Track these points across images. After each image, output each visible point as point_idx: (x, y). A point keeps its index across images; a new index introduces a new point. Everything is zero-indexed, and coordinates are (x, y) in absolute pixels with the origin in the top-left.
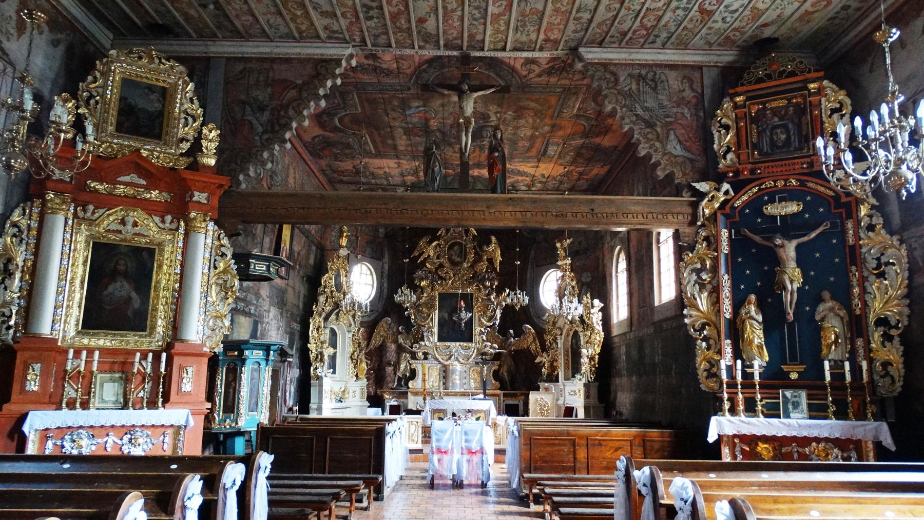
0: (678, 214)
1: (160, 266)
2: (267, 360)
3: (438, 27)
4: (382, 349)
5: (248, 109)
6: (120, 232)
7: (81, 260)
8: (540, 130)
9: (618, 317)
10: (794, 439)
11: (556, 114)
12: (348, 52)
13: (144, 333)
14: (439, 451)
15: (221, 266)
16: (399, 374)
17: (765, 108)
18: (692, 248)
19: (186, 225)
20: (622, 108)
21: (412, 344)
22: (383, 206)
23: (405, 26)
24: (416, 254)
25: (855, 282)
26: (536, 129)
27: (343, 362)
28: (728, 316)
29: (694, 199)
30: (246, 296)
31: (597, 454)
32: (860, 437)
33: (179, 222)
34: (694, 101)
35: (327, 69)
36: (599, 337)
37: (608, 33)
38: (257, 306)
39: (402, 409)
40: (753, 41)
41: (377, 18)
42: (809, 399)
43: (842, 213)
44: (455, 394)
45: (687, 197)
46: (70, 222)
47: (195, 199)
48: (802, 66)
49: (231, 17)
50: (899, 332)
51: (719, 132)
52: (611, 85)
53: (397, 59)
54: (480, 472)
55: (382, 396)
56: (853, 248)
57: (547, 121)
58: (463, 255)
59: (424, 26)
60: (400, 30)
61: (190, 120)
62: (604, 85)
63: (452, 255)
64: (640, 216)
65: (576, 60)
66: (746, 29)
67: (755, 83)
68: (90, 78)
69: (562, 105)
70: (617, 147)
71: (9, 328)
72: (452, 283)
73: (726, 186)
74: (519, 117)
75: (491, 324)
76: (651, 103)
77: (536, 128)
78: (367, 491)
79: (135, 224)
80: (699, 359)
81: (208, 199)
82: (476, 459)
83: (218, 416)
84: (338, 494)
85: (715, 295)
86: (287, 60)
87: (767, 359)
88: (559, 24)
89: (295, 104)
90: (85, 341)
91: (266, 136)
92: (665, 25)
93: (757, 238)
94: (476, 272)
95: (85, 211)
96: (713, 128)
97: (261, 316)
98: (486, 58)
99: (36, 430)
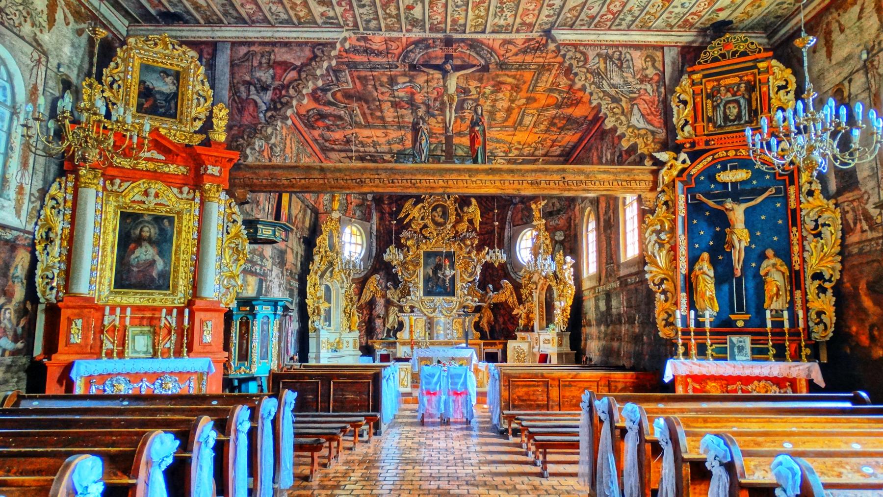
0: (640, 181)
1: (179, 233)
2: (275, 314)
3: (424, 13)
4: (371, 304)
5: (252, 88)
6: (144, 203)
7: (111, 228)
8: (516, 102)
9: (588, 273)
10: (739, 378)
11: (531, 88)
12: (341, 36)
13: (168, 292)
14: (429, 393)
15: (233, 231)
16: (388, 326)
17: (719, 84)
18: (652, 212)
19: (202, 195)
20: (590, 85)
22: (377, 176)
23: (394, 12)
24: (402, 215)
25: (795, 242)
26: (512, 101)
27: (337, 316)
28: (684, 271)
29: (655, 167)
30: (252, 257)
31: (567, 394)
32: (794, 376)
33: (195, 192)
34: (656, 78)
35: (323, 52)
36: (571, 291)
37: (577, 17)
38: (261, 266)
39: (391, 358)
40: (711, 23)
41: (369, 6)
42: (752, 344)
43: (785, 180)
44: (440, 344)
45: (648, 164)
46: (100, 195)
47: (209, 172)
48: (754, 47)
49: (236, 5)
50: (832, 284)
51: (678, 106)
52: (581, 64)
53: (387, 41)
54: (465, 411)
55: (373, 346)
56: (794, 211)
57: (523, 94)
58: (445, 214)
59: (412, 12)
60: (390, 16)
61: (202, 100)
62: (574, 63)
64: (606, 184)
65: (549, 41)
66: (702, 14)
67: (711, 62)
68: (112, 64)
69: (537, 79)
70: (587, 117)
71: (52, 288)
72: (436, 243)
73: (683, 156)
74: (499, 90)
76: (617, 80)
77: (512, 101)
78: (367, 427)
79: (157, 195)
80: (657, 311)
81: (220, 172)
82: (461, 399)
83: (234, 363)
84: (345, 428)
85: (672, 253)
86: (286, 44)
87: (718, 309)
88: (533, 10)
89: (295, 84)
90: (118, 299)
91: (269, 114)
92: (630, 11)
93: (711, 203)
94: (457, 232)
95: (112, 184)
96: (672, 103)
97: (265, 275)
98: (467, 39)
99: (81, 377)
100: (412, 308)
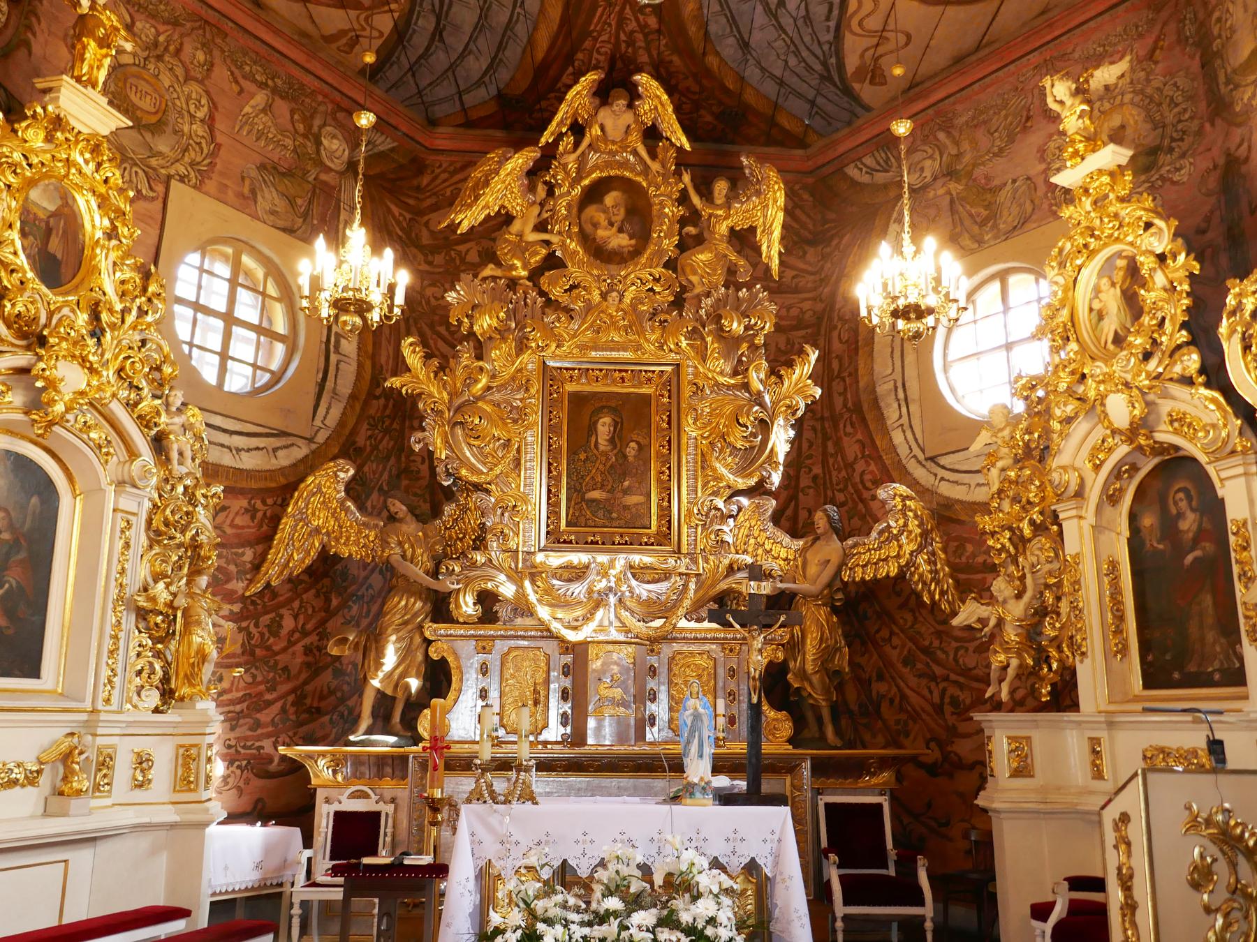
21: (437, 566)
63: (596, 226)
75: (752, 482)
100: (487, 599)
